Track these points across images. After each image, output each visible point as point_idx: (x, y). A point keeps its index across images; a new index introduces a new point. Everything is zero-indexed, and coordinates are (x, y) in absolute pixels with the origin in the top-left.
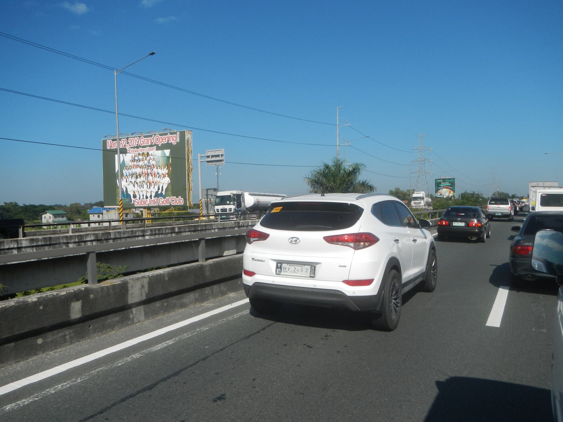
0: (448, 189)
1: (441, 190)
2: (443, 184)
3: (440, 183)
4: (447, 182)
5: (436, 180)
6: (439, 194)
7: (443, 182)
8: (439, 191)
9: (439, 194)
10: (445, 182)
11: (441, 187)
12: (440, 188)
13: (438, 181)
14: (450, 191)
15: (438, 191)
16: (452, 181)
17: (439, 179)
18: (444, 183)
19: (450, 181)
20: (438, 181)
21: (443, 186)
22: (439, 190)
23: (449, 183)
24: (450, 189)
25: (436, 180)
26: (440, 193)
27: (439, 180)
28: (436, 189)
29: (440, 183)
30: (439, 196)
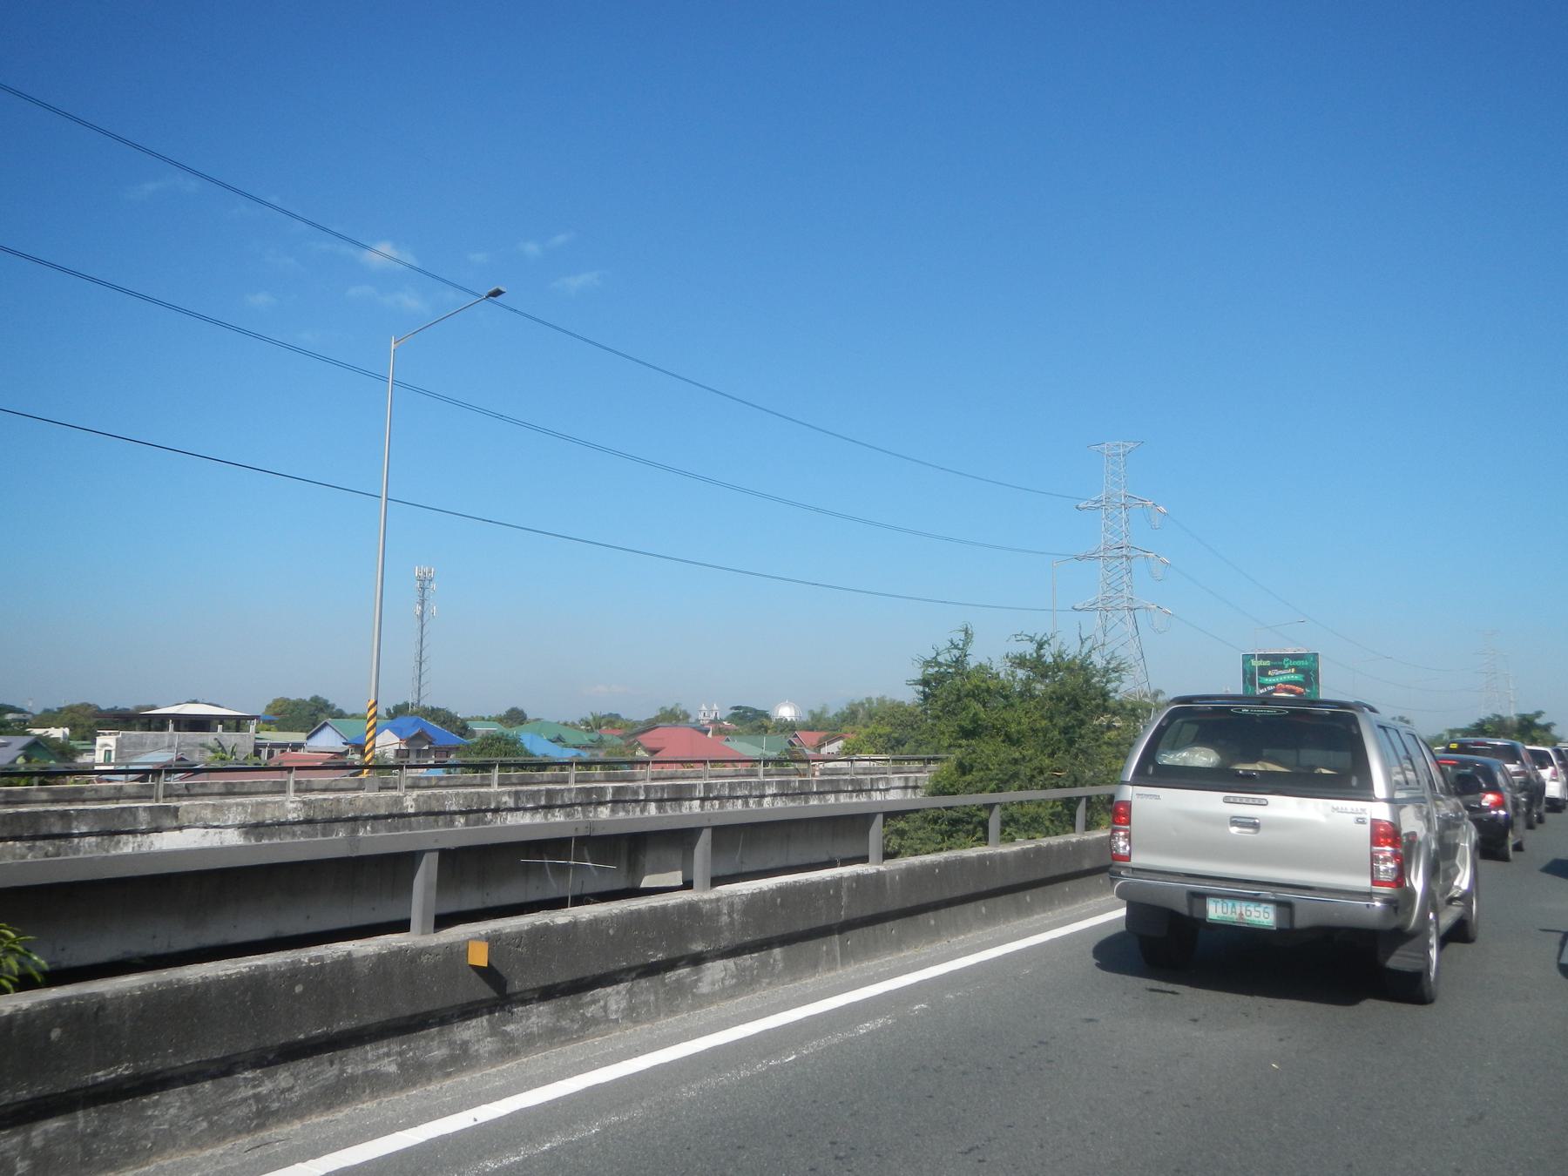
2: (1275, 676)
4: (1291, 667)
5: (1247, 658)
7: (1272, 667)
10: (1281, 668)
16: (1307, 663)
18: (1278, 672)
19: (1298, 663)
20: (1256, 663)
21: (1275, 684)
23: (1298, 670)
25: (1247, 658)
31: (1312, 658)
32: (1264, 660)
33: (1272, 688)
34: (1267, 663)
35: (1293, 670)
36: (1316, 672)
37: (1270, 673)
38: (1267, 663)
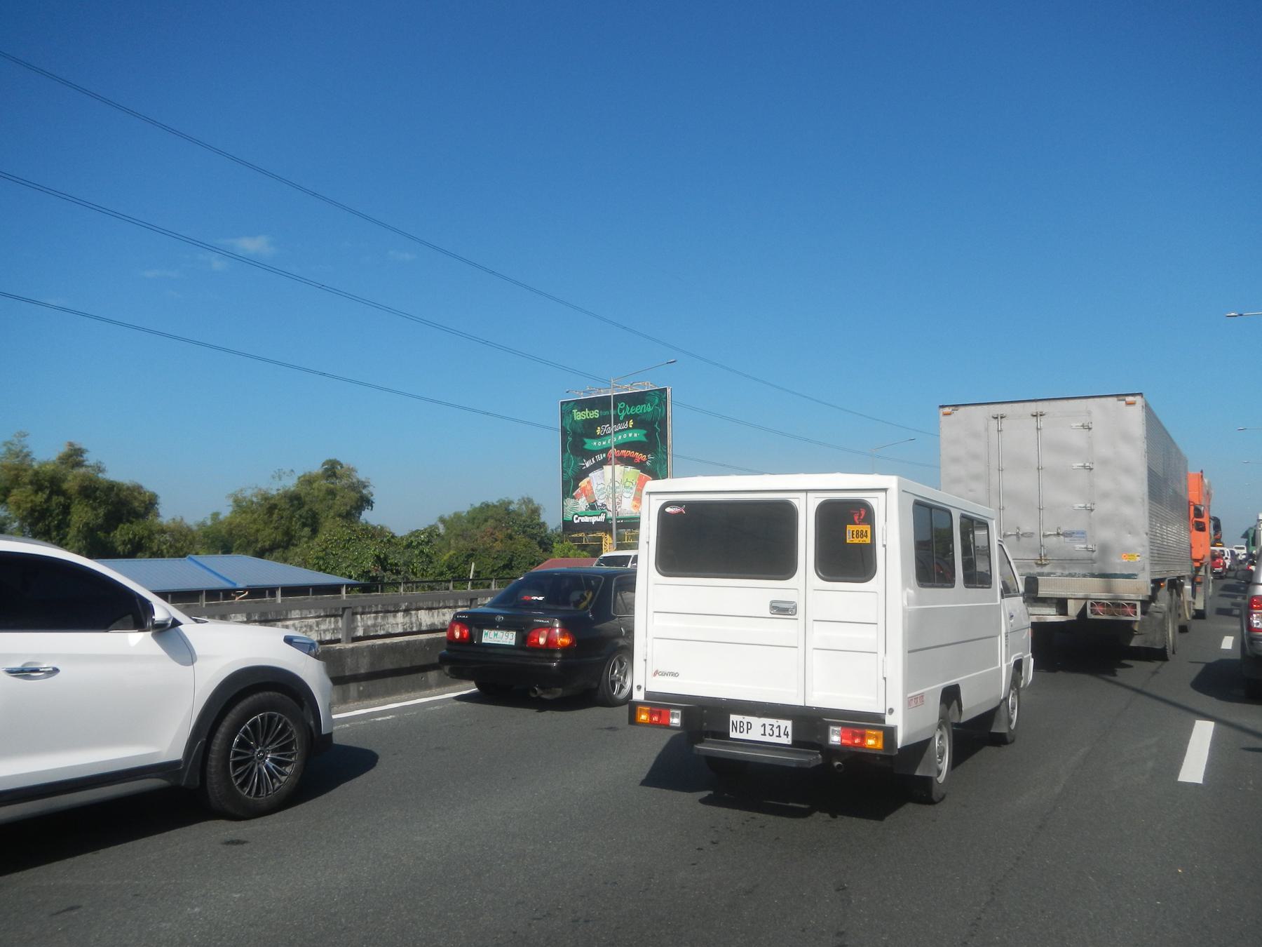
0: (629, 469)
1: (594, 476)
2: (606, 435)
3: (589, 429)
4: (627, 418)
6: (582, 504)
7: (604, 420)
8: (583, 483)
9: (582, 504)
11: (591, 454)
12: (588, 464)
13: (579, 416)
14: (641, 477)
15: (576, 487)
16: (650, 409)
17: (583, 405)
19: (639, 409)
20: (579, 416)
21: (606, 450)
22: (584, 473)
23: (640, 423)
24: (640, 466)
26: (588, 493)
27: (582, 410)
28: (570, 472)
29: (589, 429)
30: (586, 519)
31: (657, 401)
32: (591, 409)
33: (600, 457)
34: (595, 414)
35: (631, 423)
36: (663, 423)
37: (598, 432)
38: (595, 414)
